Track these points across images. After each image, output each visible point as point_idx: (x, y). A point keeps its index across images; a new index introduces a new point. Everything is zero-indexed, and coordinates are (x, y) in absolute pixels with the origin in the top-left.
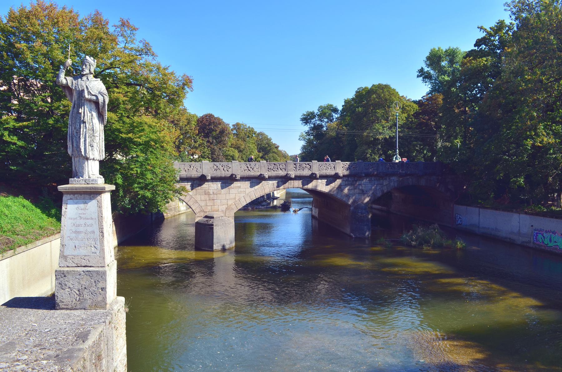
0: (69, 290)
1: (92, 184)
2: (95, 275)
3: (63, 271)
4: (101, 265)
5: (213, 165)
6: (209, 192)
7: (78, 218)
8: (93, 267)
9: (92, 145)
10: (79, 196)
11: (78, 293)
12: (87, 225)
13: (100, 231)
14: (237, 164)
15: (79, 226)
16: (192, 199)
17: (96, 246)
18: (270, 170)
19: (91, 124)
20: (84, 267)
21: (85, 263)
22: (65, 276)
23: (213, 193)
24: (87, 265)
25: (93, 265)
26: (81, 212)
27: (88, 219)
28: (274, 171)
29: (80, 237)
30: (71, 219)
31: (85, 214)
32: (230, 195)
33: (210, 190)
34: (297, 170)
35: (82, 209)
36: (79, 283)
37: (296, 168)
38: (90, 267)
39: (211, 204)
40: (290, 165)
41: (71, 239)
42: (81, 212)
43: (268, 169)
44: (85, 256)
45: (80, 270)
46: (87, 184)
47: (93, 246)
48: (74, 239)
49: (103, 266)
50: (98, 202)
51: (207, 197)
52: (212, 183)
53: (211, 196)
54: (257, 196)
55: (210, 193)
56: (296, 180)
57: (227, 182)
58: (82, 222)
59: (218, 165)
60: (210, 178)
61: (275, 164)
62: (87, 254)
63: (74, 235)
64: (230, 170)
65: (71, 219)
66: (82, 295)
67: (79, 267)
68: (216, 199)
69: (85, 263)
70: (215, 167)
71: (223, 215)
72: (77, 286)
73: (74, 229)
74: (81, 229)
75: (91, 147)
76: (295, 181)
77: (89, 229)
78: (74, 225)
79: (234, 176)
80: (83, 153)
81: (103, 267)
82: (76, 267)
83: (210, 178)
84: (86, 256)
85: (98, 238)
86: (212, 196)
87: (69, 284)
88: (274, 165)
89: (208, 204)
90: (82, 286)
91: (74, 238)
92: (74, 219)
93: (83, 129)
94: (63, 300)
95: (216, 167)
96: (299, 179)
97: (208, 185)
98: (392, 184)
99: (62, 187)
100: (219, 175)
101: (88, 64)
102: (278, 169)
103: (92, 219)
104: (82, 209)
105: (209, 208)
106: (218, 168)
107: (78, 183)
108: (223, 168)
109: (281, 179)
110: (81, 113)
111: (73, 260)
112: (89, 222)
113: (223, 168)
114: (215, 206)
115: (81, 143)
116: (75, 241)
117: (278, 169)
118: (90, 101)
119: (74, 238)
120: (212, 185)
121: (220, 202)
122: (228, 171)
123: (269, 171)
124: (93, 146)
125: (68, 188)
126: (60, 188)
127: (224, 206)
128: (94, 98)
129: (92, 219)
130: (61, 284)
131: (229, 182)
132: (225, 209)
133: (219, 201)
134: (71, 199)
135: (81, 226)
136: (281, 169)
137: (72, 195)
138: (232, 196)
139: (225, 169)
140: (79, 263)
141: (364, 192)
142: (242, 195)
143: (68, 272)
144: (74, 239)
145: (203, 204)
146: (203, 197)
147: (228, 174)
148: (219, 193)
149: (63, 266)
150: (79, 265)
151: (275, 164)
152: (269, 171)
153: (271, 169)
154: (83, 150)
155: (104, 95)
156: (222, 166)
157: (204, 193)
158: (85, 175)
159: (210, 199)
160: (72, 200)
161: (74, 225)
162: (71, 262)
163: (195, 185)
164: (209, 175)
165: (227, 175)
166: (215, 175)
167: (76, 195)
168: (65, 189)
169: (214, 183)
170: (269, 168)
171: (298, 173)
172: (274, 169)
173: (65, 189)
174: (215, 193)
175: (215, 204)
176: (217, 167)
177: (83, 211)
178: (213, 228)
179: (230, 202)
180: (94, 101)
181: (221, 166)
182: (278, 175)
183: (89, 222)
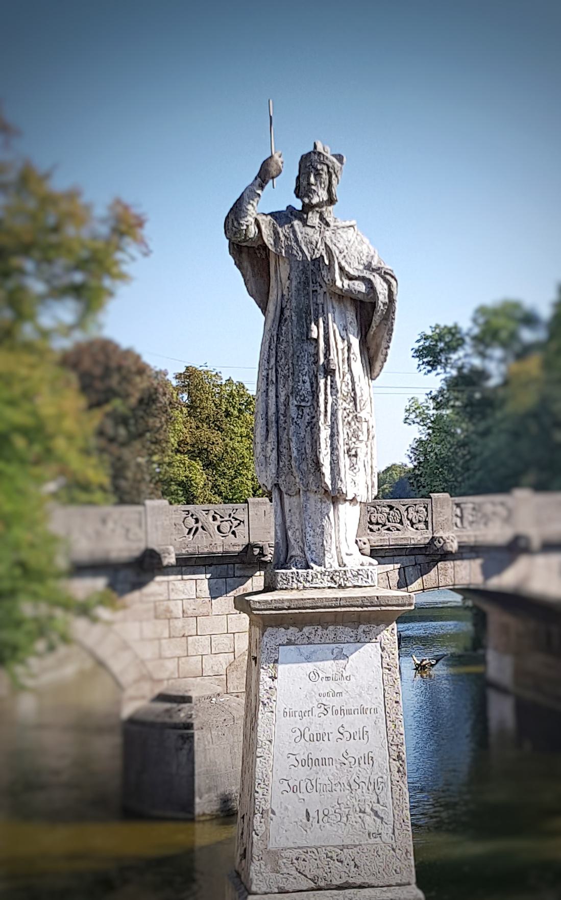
1: (355, 587)
5: (184, 515)
6: (168, 610)
7: (316, 711)
9: (353, 452)
10: (319, 632)
12: (347, 735)
13: (392, 753)
14: (263, 508)
15: (319, 737)
17: (377, 807)
18: (375, 527)
19: (348, 376)
20: (339, 888)
21: (343, 874)
23: (183, 612)
24: (351, 881)
26: (324, 686)
27: (349, 712)
28: (388, 529)
33: (171, 605)
34: (466, 524)
37: (462, 518)
38: (361, 887)
39: (179, 652)
40: (442, 507)
42: (324, 686)
43: (371, 523)
44: (343, 847)
46: (340, 586)
47: (368, 810)
49: (404, 881)
50: (383, 649)
51: (162, 628)
52: (179, 577)
55: (174, 615)
56: (462, 559)
57: (231, 572)
59: (202, 516)
61: (391, 508)
62: (348, 842)
63: (302, 773)
64: (242, 530)
67: (320, 889)
69: (343, 874)
70: (191, 522)
71: (220, 689)
73: (302, 749)
74: (325, 749)
75: (349, 456)
76: (458, 562)
77: (357, 748)
78: (302, 735)
79: (257, 551)
80: (328, 480)
81: (404, 885)
82: (313, 890)
86: (179, 623)
88: (387, 510)
89: (167, 653)
91: (303, 785)
92: (303, 715)
93: (326, 394)
95: (193, 521)
96: (473, 555)
97: (164, 586)
99: (266, 602)
100: (206, 550)
101: (325, 168)
102: (401, 522)
103: (363, 711)
105: (171, 665)
106: (200, 525)
107: (307, 585)
108: (217, 523)
110: (317, 340)
113: (217, 523)
115: (323, 445)
116: (306, 796)
117: (401, 522)
118: (342, 296)
120: (180, 585)
121: (208, 643)
122: (234, 533)
123: (371, 530)
124: (356, 455)
125: (286, 605)
126: (257, 606)
128: (361, 287)
129: (363, 711)
131: (238, 573)
133: (205, 640)
134: (290, 643)
135: (326, 738)
136: (412, 524)
137: (292, 630)
139: (226, 527)
140: (320, 872)
145: (147, 652)
146: (150, 628)
147: (235, 544)
148: (205, 611)
149: (264, 889)
150: (322, 884)
151: (391, 508)
152: (371, 530)
153: (378, 524)
154: (326, 470)
155: (388, 277)
156: (214, 519)
157: (152, 614)
158: (328, 555)
159: (173, 634)
160: (292, 647)
161: (302, 735)
162: (294, 872)
164: (171, 548)
165: (232, 549)
166: (191, 550)
167: (306, 630)
168: (276, 609)
169: (185, 577)
170: (374, 520)
172: (389, 525)
173: (276, 609)
174: (190, 612)
175: (191, 652)
176: (197, 521)
177: (332, 685)
178: (192, 736)
180: (360, 297)
181: (211, 519)
182: (404, 542)
183: (354, 723)
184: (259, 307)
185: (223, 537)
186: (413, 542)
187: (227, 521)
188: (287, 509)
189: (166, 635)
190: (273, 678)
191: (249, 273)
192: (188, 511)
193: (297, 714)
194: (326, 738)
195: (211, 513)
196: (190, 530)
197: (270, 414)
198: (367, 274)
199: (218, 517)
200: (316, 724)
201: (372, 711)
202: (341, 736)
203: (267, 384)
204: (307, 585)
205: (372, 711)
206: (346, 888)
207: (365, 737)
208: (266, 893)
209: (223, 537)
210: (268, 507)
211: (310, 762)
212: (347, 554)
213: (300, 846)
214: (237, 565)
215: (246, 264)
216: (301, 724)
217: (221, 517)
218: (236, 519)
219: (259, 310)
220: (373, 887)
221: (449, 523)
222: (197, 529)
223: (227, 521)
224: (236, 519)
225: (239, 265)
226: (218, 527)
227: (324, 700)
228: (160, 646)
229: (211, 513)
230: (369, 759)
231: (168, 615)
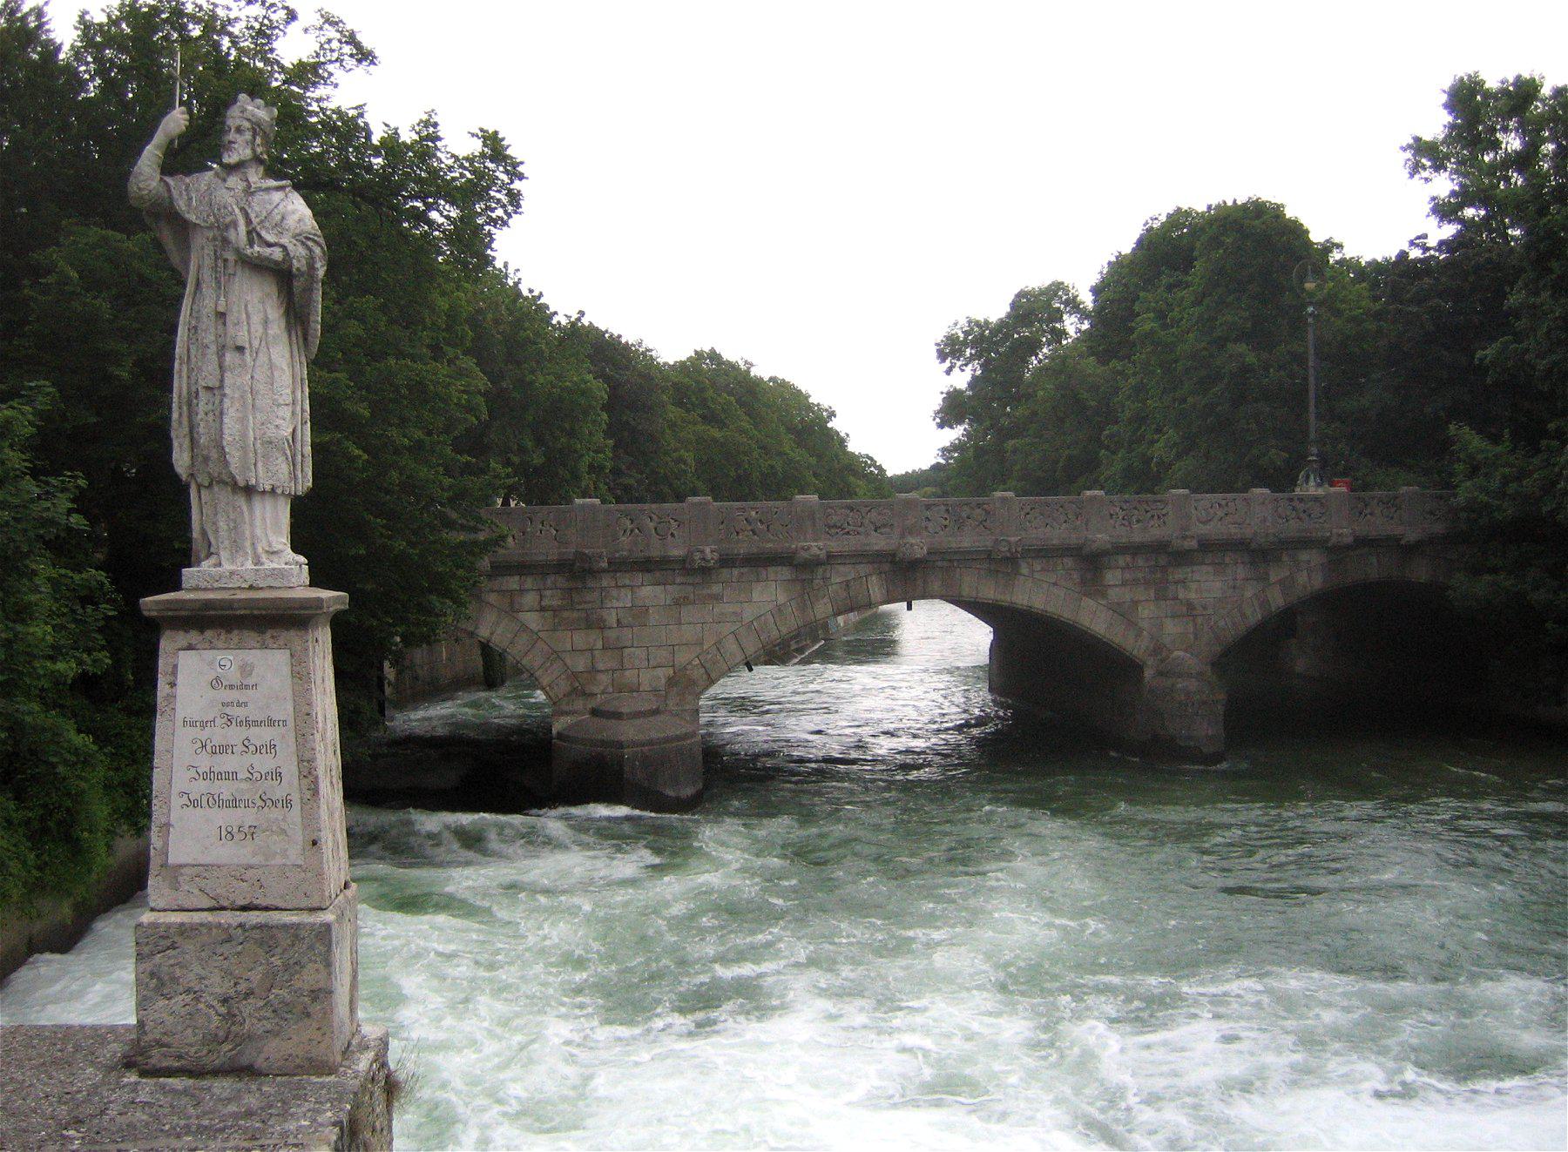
0: (188, 998)
2: (284, 939)
3: (169, 926)
4: (305, 903)
8: (277, 909)
11: (223, 1010)
12: (252, 748)
15: (223, 749)
16: (540, 644)
18: (833, 531)
20: (244, 908)
22: (173, 947)
24: (256, 902)
25: (281, 904)
27: (257, 724)
29: (226, 796)
30: (193, 724)
31: (246, 704)
32: (684, 627)
33: (604, 613)
35: (231, 687)
36: (227, 973)
38: (267, 909)
39: (614, 664)
41: (195, 804)
45: (230, 921)
48: (204, 803)
49: (315, 905)
53: (608, 633)
54: (784, 630)
58: (235, 735)
60: (604, 565)
62: (254, 861)
65: (193, 724)
66: (239, 1018)
67: (223, 908)
68: (629, 644)
72: (218, 985)
73: (204, 761)
74: (228, 763)
77: (264, 763)
78: (204, 746)
83: (604, 565)
84: (251, 867)
85: (296, 798)
86: (612, 634)
87: (190, 979)
89: (601, 666)
90: (236, 984)
92: (204, 724)
94: (166, 1039)
95: (628, 522)
98: (1302, 578)
104: (231, 687)
111: (203, 883)
112: (261, 735)
114: (627, 673)
119: (204, 799)
121: (644, 656)
127: (660, 672)
128: (277, 254)
129: (271, 722)
130: (159, 979)
131: (678, 580)
132: (663, 681)
134: (190, 648)
135: (229, 751)
138: (689, 632)
141: (1194, 609)
142: (726, 629)
143: (183, 929)
144: (204, 803)
153: (835, 526)
155: (310, 243)
161: (204, 746)
162: (196, 891)
163: (548, 593)
175: (627, 665)
177: (234, 695)
179: (683, 657)
183: (261, 735)
188: (203, 502)
189: (599, 645)
190: (173, 685)
193: (198, 724)
194: (229, 751)
198: (284, 241)
199: (654, 517)
200: (218, 735)
201: (281, 723)
202: (246, 749)
204: (216, 585)
205: (281, 723)
206: (251, 909)
207: (273, 751)
208: (165, 910)
211: (211, 775)
212: (267, 552)
213: (202, 862)
216: (203, 735)
220: (282, 909)
222: (632, 531)
227: (228, 710)
228: (593, 657)
230: (277, 775)
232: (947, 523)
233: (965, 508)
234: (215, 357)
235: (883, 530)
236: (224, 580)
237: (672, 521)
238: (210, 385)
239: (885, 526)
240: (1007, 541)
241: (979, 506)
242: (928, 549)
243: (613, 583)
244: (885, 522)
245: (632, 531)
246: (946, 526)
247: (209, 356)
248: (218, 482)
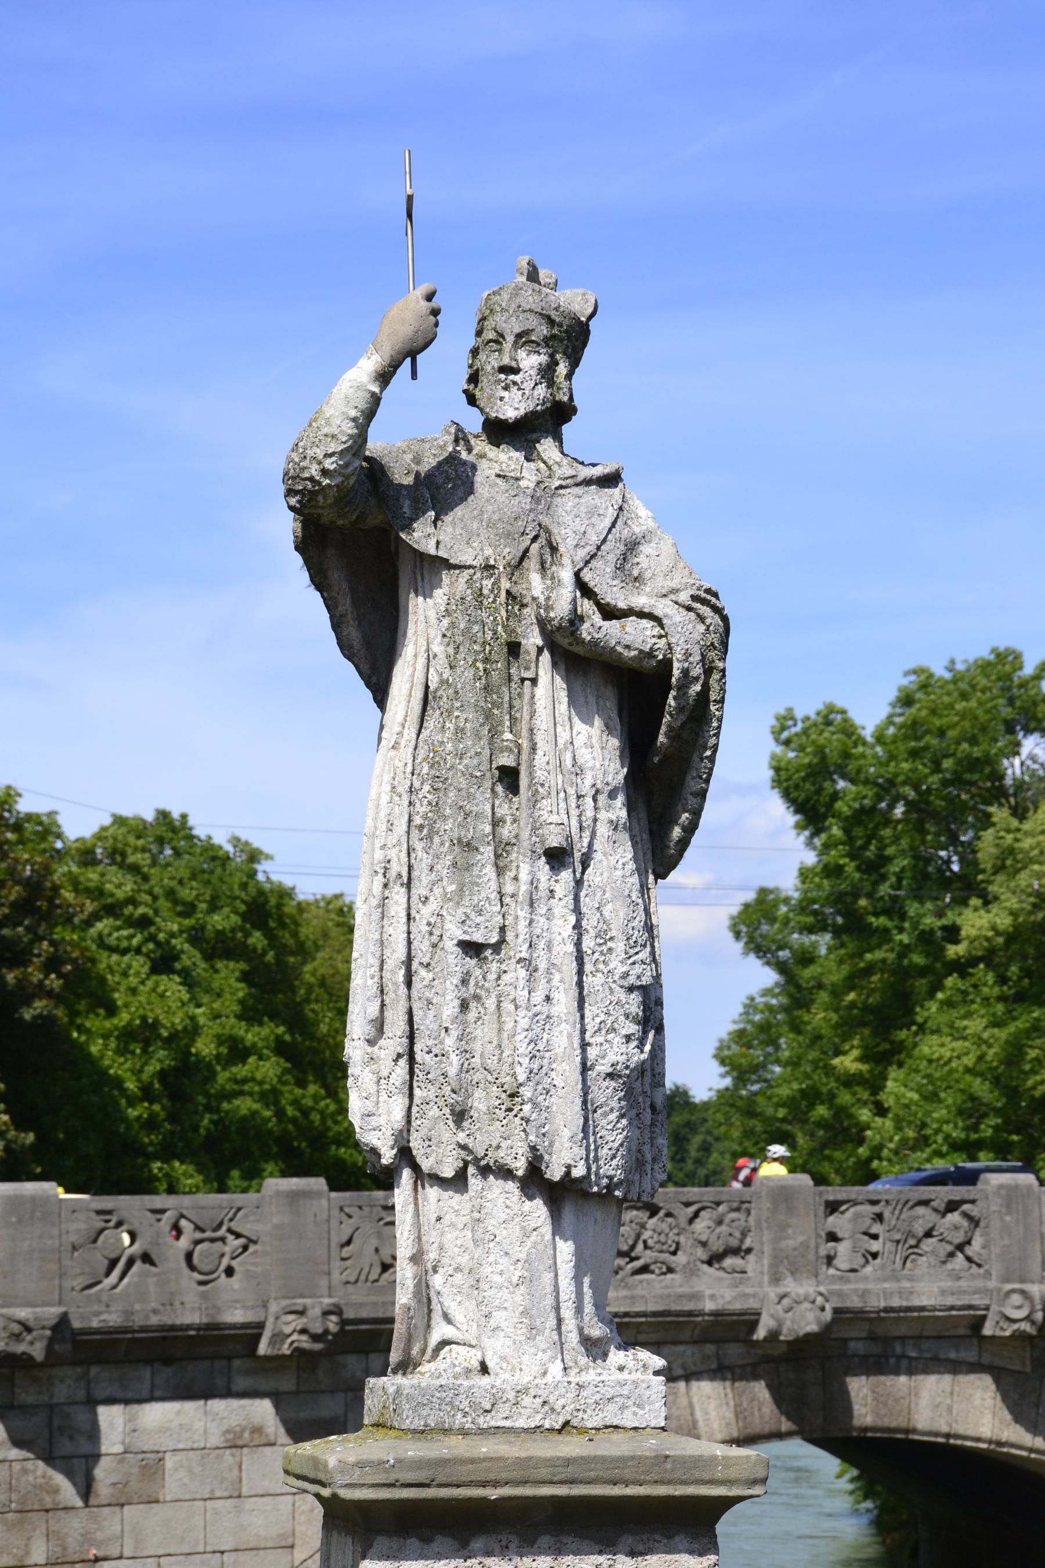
28: (645, 1269)
100: (154, 1320)
109: (710, 1349)
113: (184, 1243)
166: (113, 1319)
171: (864, 1294)
172: (647, 1257)
184: (368, 685)
185: (202, 1283)
186: (709, 1306)
187: (213, 1240)
191: (346, 605)
192: (109, 1212)
195: (169, 1217)
196: (113, 1263)
197: (390, 964)
203: (386, 886)
204: (484, 1422)
209: (202, 1283)
210: (324, 1202)
214: (237, 1363)
215: (336, 576)
217: (198, 1228)
218: (238, 1236)
219: (368, 694)
221: (811, 1256)
222: (131, 1262)
223: (213, 1240)
224: (238, 1236)
225: (319, 581)
226: (189, 1256)
229: (169, 1217)
231: (48, 1501)
232: (875, 1246)
233: (921, 1210)
234: (490, 871)
235: (729, 1262)
236: (504, 1410)
237: (230, 1237)
238: (478, 937)
239: (735, 1251)
240: (1023, 1292)
241: (952, 1206)
242: (836, 1311)
243: (81, 1395)
244: (734, 1243)
245: (131, 1262)
246: (875, 1255)
247: (476, 871)
248: (485, 1171)
